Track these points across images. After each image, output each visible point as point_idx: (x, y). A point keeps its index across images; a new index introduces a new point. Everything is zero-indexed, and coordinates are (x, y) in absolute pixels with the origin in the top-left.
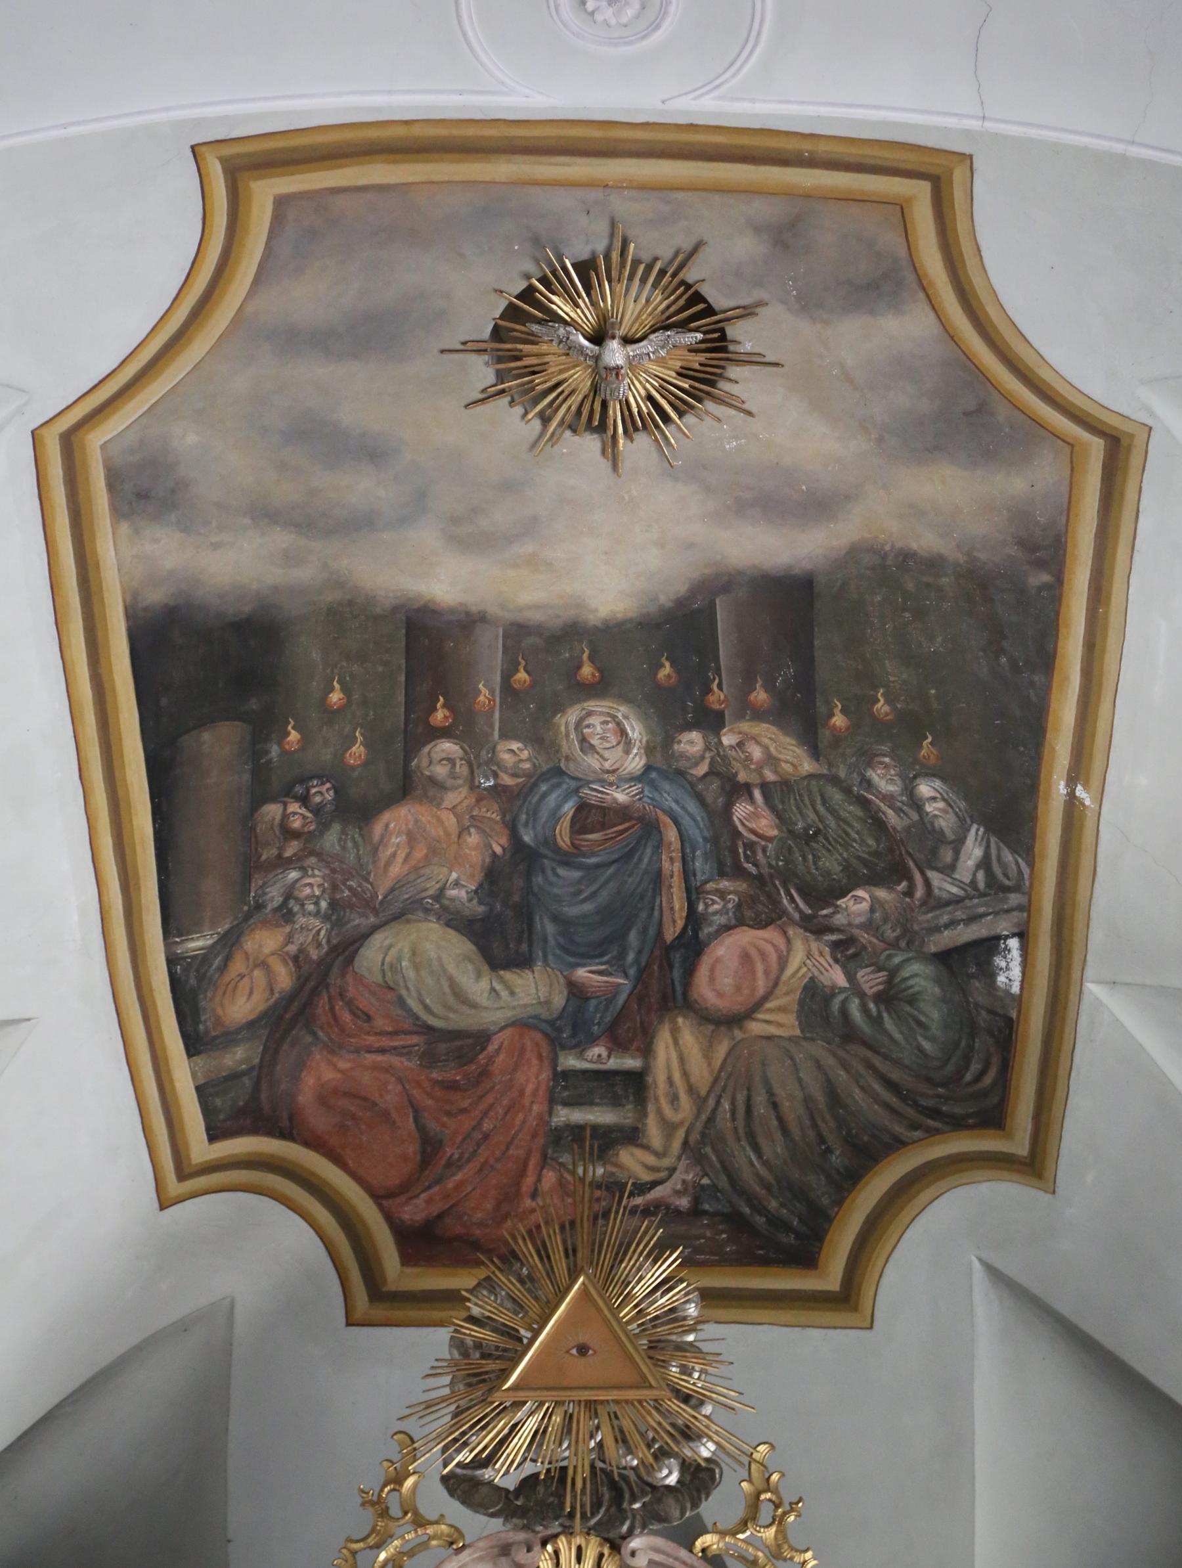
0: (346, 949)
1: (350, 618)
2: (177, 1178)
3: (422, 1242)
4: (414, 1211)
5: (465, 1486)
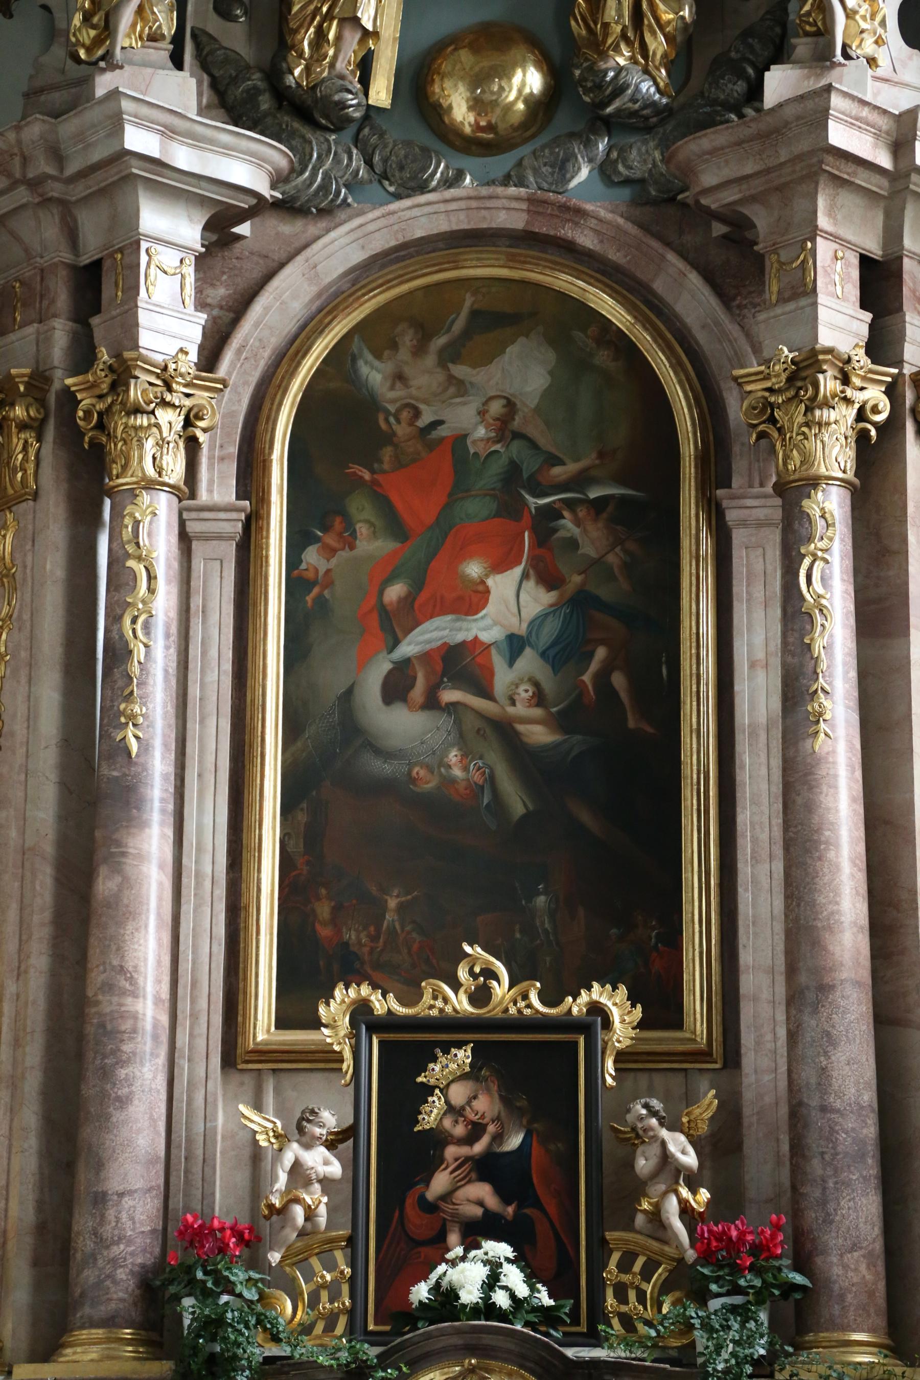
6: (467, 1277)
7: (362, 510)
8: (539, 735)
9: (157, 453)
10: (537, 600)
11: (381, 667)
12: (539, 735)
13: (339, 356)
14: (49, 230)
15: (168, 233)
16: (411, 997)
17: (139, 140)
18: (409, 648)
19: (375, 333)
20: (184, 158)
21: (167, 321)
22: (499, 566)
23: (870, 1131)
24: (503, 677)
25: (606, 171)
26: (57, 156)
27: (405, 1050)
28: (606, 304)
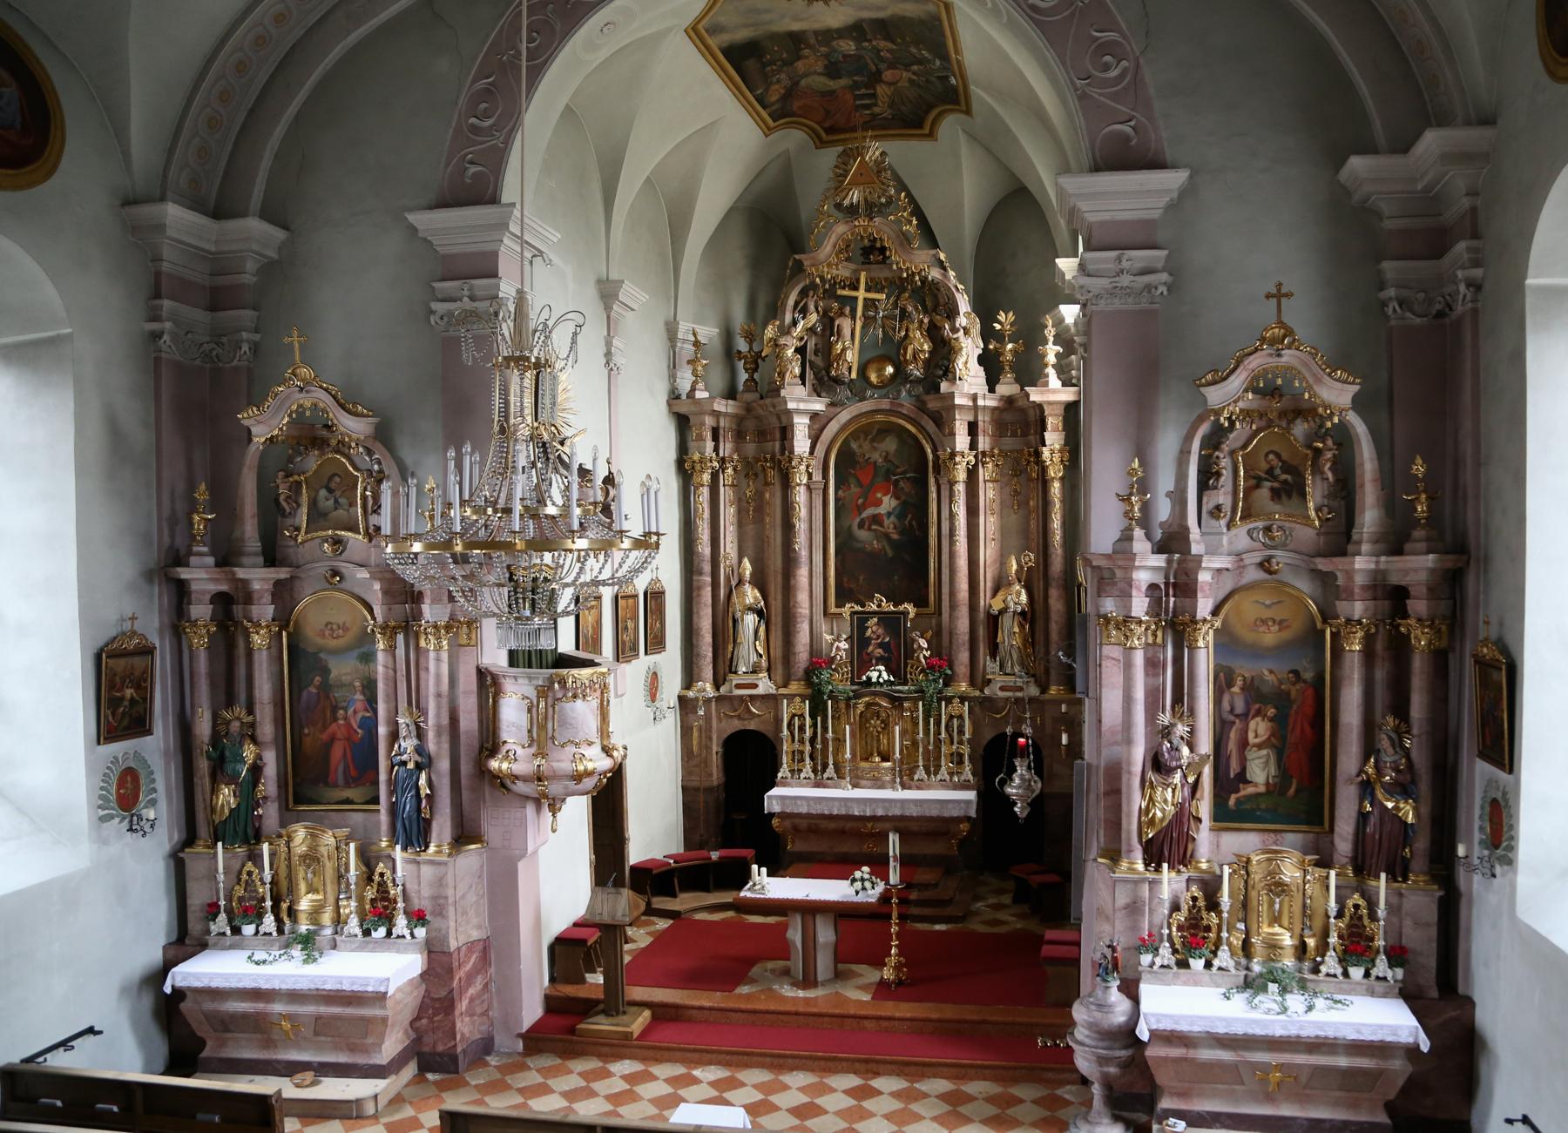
0: (797, 83)
1: (774, 37)
2: (768, 131)
3: (829, 131)
4: (827, 125)
5: (838, 206)
6: (874, 675)
8: (895, 537)
9: (801, 478)
10: (894, 503)
12: (895, 537)
13: (846, 442)
14: (774, 420)
15: (801, 426)
17: (791, 405)
18: (864, 515)
19: (854, 435)
20: (802, 406)
21: (801, 444)
23: (967, 638)
24: (886, 522)
25: (909, 392)
27: (861, 620)
28: (910, 427)
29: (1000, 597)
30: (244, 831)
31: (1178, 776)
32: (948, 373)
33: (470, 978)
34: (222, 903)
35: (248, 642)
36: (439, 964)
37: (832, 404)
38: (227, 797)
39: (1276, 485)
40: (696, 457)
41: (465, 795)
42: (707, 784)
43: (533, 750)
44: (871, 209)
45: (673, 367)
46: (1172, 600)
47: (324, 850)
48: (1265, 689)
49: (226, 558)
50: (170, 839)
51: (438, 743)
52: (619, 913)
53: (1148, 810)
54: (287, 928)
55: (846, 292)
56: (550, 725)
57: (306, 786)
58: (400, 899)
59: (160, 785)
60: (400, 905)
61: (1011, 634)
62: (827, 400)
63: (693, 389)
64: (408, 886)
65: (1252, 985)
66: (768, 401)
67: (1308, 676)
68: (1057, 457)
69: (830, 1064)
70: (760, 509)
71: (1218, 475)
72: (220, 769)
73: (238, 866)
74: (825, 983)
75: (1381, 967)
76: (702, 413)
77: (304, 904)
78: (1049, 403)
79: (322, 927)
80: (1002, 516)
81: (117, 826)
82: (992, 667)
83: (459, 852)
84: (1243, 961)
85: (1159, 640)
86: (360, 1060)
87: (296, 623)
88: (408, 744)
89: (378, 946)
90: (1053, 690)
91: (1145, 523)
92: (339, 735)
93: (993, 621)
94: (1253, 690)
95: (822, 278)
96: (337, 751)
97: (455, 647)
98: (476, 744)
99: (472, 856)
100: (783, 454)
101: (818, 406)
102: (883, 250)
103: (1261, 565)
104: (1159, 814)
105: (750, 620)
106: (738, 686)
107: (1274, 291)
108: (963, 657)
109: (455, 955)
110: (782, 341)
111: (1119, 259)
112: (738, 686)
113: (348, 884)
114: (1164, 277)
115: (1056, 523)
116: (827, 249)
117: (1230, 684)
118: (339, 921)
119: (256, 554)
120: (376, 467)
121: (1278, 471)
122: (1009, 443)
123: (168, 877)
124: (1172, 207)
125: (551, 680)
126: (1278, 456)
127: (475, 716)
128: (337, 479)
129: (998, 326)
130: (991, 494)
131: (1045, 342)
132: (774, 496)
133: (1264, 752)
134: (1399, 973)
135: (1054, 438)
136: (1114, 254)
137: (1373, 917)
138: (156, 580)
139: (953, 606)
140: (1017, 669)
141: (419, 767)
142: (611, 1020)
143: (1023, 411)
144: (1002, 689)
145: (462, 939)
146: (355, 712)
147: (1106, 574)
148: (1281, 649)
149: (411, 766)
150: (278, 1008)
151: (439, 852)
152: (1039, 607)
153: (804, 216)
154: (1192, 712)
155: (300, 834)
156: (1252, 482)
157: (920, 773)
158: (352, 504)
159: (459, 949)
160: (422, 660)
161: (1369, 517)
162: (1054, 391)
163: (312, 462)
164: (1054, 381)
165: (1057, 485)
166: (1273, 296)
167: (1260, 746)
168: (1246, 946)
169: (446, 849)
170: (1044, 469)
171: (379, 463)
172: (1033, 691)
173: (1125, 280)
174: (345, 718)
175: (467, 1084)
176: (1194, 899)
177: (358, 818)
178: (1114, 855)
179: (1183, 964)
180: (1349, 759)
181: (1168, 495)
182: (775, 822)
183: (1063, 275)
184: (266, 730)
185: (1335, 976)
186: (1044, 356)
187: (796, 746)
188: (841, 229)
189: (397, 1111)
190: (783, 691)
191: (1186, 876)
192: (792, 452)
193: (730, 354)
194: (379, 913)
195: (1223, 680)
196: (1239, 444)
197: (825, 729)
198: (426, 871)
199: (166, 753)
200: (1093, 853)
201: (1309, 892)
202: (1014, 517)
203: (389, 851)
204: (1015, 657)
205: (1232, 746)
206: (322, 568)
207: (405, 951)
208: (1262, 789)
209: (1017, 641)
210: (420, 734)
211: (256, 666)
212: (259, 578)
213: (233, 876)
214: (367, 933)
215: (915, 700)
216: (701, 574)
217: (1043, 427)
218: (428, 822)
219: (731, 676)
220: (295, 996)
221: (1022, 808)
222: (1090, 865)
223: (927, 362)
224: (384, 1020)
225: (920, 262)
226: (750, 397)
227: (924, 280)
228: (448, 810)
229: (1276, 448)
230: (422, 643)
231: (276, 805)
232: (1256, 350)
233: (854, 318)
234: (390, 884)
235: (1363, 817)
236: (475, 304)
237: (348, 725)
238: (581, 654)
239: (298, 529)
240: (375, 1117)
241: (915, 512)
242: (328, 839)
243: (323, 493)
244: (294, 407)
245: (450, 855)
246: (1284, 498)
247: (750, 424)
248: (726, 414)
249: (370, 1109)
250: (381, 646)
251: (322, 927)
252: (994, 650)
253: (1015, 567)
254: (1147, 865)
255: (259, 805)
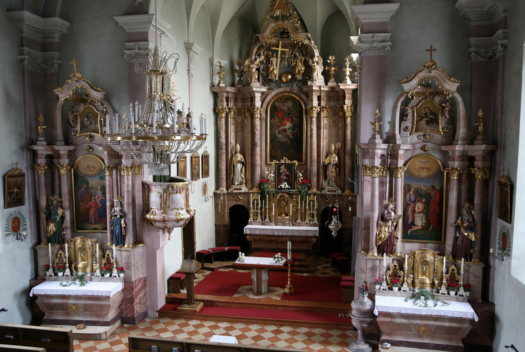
5: (272, 17)
7: (276, 116)
8: (291, 137)
10: (291, 125)
11: (278, 131)
12: (291, 137)
13: (274, 103)
14: (248, 95)
15: (258, 96)
16: (279, 161)
17: (254, 89)
18: (280, 129)
19: (277, 100)
20: (258, 90)
21: (258, 103)
22: (288, 122)
23: (316, 173)
24: (288, 132)
25: (297, 85)
26: (248, 89)
27: (278, 166)
28: (297, 97)
29: (328, 158)
30: (58, 239)
31: (390, 223)
32: (311, 78)
33: (140, 291)
34: (51, 265)
35: (59, 172)
36: (128, 287)
37: (269, 89)
38: (52, 227)
39: (428, 119)
40: (220, 107)
41: (138, 227)
42: (224, 224)
43: (162, 211)
44: (284, 18)
45: (212, 75)
46: (389, 160)
47: (87, 246)
48: (422, 192)
49: (51, 142)
50: (32, 242)
51: (128, 209)
52: (192, 269)
53: (379, 234)
54: (74, 274)
55: (274, 48)
56: (168, 202)
57: (80, 224)
58: (115, 264)
59: (28, 223)
60: (115, 265)
61: (332, 172)
62: (267, 87)
63: (219, 83)
64: (117, 259)
65: (415, 297)
66: (246, 88)
67: (438, 188)
68: (349, 109)
69: (266, 322)
70: (243, 127)
71: (407, 115)
72: (50, 218)
73: (56, 252)
74: (264, 294)
75: (461, 291)
76: (222, 92)
77: (80, 265)
78: (347, 89)
79: (87, 273)
80: (329, 130)
81: (12, 238)
82: (325, 183)
83: (135, 247)
84: (412, 288)
85: (384, 174)
86: (101, 320)
87: (77, 165)
88: (117, 209)
89: (107, 280)
90: (346, 192)
91: (380, 132)
92: (93, 206)
93: (326, 167)
94: (417, 192)
95: (266, 43)
96: (92, 212)
97: (134, 175)
98: (142, 209)
99: (140, 249)
100: (251, 107)
101: (264, 89)
102: (288, 33)
103: (421, 148)
104: (383, 236)
105: (239, 166)
106: (235, 189)
107: (429, 49)
108: (315, 180)
109: (134, 283)
110: (251, 66)
111: (373, 37)
112: (235, 189)
113: (96, 258)
114: (389, 43)
115: (349, 132)
116: (268, 32)
117: (409, 191)
118: (93, 271)
119: (61, 141)
120: (105, 110)
121: (429, 114)
122: (332, 103)
123: (31, 255)
124: (393, 17)
125: (168, 187)
126: (429, 109)
127: (141, 199)
128: (91, 114)
129: (329, 61)
130: (325, 122)
131: (346, 67)
132: (248, 122)
133: (421, 215)
134: (468, 293)
135: (348, 102)
136: (371, 35)
137: (459, 273)
138: (25, 150)
139: (311, 162)
140: (334, 184)
141: (121, 217)
142: (189, 306)
143: (337, 92)
144: (328, 191)
145: (137, 278)
146: (98, 197)
147: (366, 151)
148: (428, 178)
149: (118, 216)
150: (71, 301)
151: (128, 247)
152: (342, 162)
153: (259, 20)
154: (396, 200)
155: (79, 241)
156: (419, 118)
157: (299, 221)
158: (96, 123)
159: (135, 281)
160: (122, 179)
161: (461, 131)
162: (349, 85)
163: (81, 108)
164: (349, 81)
165: (349, 119)
166: (429, 50)
167: (419, 213)
168: (413, 283)
169: (131, 246)
170: (344, 113)
171: (106, 108)
172: (339, 192)
173: (375, 44)
174: (95, 200)
175: (139, 328)
176: (395, 266)
177: (100, 235)
178: (367, 250)
179: (391, 289)
180: (452, 217)
181: (389, 122)
182: (248, 237)
183: (353, 42)
184: (66, 204)
185: (445, 294)
186: (345, 72)
187: (255, 211)
188: (273, 25)
189: (113, 337)
190: (251, 191)
191: (392, 258)
192: (254, 106)
193: (232, 70)
194: (107, 268)
195: (407, 189)
196: (415, 104)
197: (265, 205)
198: (124, 254)
199: (30, 212)
200: (359, 250)
201: (436, 264)
202: (333, 130)
203: (111, 246)
204: (333, 180)
205: (410, 212)
206: (86, 146)
207: (116, 282)
208: (420, 228)
209: (334, 174)
210: (122, 205)
211: (62, 181)
212: (63, 149)
213: (55, 255)
214: (103, 275)
215: (298, 195)
216: (222, 149)
217: (344, 98)
218: (124, 237)
219: (232, 186)
220: (77, 297)
221: (335, 233)
222: (358, 254)
223: (303, 74)
224: (109, 306)
225: (301, 37)
226: (239, 86)
227: (302, 44)
228: (132, 232)
229: (428, 106)
230: (122, 173)
231: (70, 230)
232: (422, 70)
233: (277, 58)
234: (111, 258)
235: (456, 238)
236: (140, 51)
237: (96, 202)
238: (179, 178)
239: (77, 132)
240: (106, 340)
241: (298, 128)
242: (89, 242)
243: (86, 119)
244: (75, 88)
245: (132, 248)
246: (431, 123)
247: (240, 96)
248: (231, 92)
249: (104, 337)
250: (107, 174)
251: (87, 273)
252: (326, 177)
253: (333, 148)
254: (378, 254)
255: (64, 230)
